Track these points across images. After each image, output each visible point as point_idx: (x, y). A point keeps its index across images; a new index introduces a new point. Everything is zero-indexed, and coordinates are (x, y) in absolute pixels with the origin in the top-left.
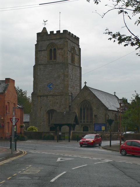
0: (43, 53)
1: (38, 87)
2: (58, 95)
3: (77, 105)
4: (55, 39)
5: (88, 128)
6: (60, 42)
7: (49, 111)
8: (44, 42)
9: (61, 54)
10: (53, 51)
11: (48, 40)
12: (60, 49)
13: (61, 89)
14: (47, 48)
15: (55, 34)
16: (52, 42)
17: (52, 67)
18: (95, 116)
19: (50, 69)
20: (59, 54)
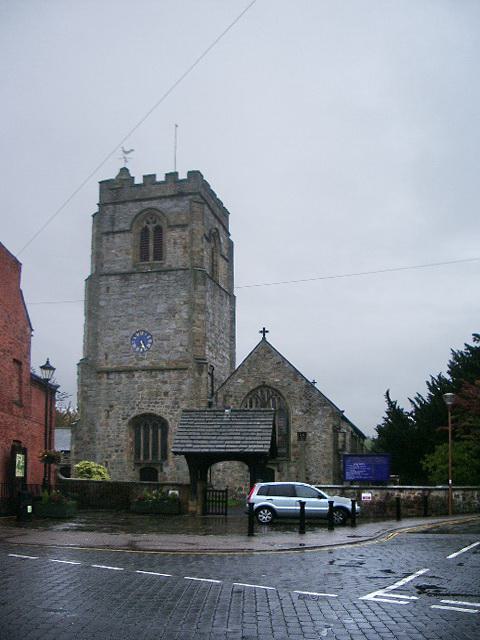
0: (118, 239)
1: (99, 344)
2: (169, 370)
3: (235, 400)
4: (160, 198)
6: (176, 206)
7: (136, 417)
11: (137, 200)
12: (178, 226)
14: (131, 226)
15: (159, 183)
16: (149, 206)
18: (302, 436)
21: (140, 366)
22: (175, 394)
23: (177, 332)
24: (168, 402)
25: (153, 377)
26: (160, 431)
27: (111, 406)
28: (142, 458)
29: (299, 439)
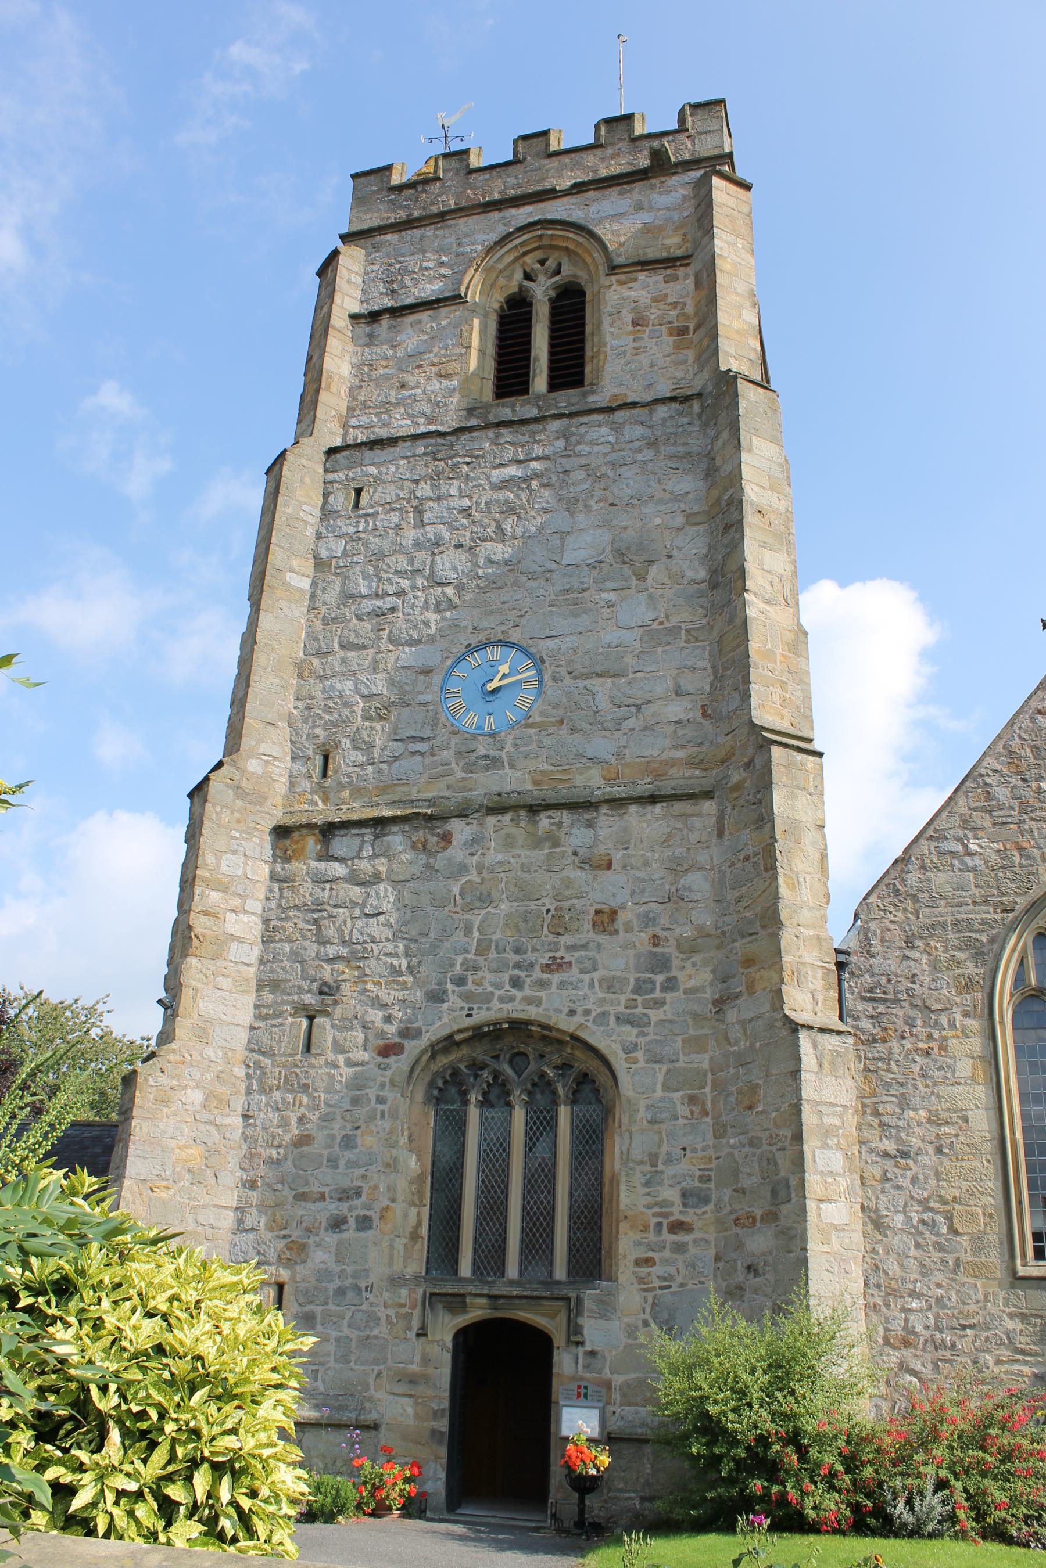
2: (617, 803)
4: (579, 188)
6: (639, 207)
7: (449, 1043)
8: (429, 232)
9: (653, 314)
13: (676, 710)
17: (538, 450)
19: (497, 475)
20: (628, 317)
21: (478, 794)
22: (648, 920)
23: (658, 635)
24: (618, 957)
25: (537, 843)
26: (564, 1113)
27: (327, 990)
28: (466, 1269)
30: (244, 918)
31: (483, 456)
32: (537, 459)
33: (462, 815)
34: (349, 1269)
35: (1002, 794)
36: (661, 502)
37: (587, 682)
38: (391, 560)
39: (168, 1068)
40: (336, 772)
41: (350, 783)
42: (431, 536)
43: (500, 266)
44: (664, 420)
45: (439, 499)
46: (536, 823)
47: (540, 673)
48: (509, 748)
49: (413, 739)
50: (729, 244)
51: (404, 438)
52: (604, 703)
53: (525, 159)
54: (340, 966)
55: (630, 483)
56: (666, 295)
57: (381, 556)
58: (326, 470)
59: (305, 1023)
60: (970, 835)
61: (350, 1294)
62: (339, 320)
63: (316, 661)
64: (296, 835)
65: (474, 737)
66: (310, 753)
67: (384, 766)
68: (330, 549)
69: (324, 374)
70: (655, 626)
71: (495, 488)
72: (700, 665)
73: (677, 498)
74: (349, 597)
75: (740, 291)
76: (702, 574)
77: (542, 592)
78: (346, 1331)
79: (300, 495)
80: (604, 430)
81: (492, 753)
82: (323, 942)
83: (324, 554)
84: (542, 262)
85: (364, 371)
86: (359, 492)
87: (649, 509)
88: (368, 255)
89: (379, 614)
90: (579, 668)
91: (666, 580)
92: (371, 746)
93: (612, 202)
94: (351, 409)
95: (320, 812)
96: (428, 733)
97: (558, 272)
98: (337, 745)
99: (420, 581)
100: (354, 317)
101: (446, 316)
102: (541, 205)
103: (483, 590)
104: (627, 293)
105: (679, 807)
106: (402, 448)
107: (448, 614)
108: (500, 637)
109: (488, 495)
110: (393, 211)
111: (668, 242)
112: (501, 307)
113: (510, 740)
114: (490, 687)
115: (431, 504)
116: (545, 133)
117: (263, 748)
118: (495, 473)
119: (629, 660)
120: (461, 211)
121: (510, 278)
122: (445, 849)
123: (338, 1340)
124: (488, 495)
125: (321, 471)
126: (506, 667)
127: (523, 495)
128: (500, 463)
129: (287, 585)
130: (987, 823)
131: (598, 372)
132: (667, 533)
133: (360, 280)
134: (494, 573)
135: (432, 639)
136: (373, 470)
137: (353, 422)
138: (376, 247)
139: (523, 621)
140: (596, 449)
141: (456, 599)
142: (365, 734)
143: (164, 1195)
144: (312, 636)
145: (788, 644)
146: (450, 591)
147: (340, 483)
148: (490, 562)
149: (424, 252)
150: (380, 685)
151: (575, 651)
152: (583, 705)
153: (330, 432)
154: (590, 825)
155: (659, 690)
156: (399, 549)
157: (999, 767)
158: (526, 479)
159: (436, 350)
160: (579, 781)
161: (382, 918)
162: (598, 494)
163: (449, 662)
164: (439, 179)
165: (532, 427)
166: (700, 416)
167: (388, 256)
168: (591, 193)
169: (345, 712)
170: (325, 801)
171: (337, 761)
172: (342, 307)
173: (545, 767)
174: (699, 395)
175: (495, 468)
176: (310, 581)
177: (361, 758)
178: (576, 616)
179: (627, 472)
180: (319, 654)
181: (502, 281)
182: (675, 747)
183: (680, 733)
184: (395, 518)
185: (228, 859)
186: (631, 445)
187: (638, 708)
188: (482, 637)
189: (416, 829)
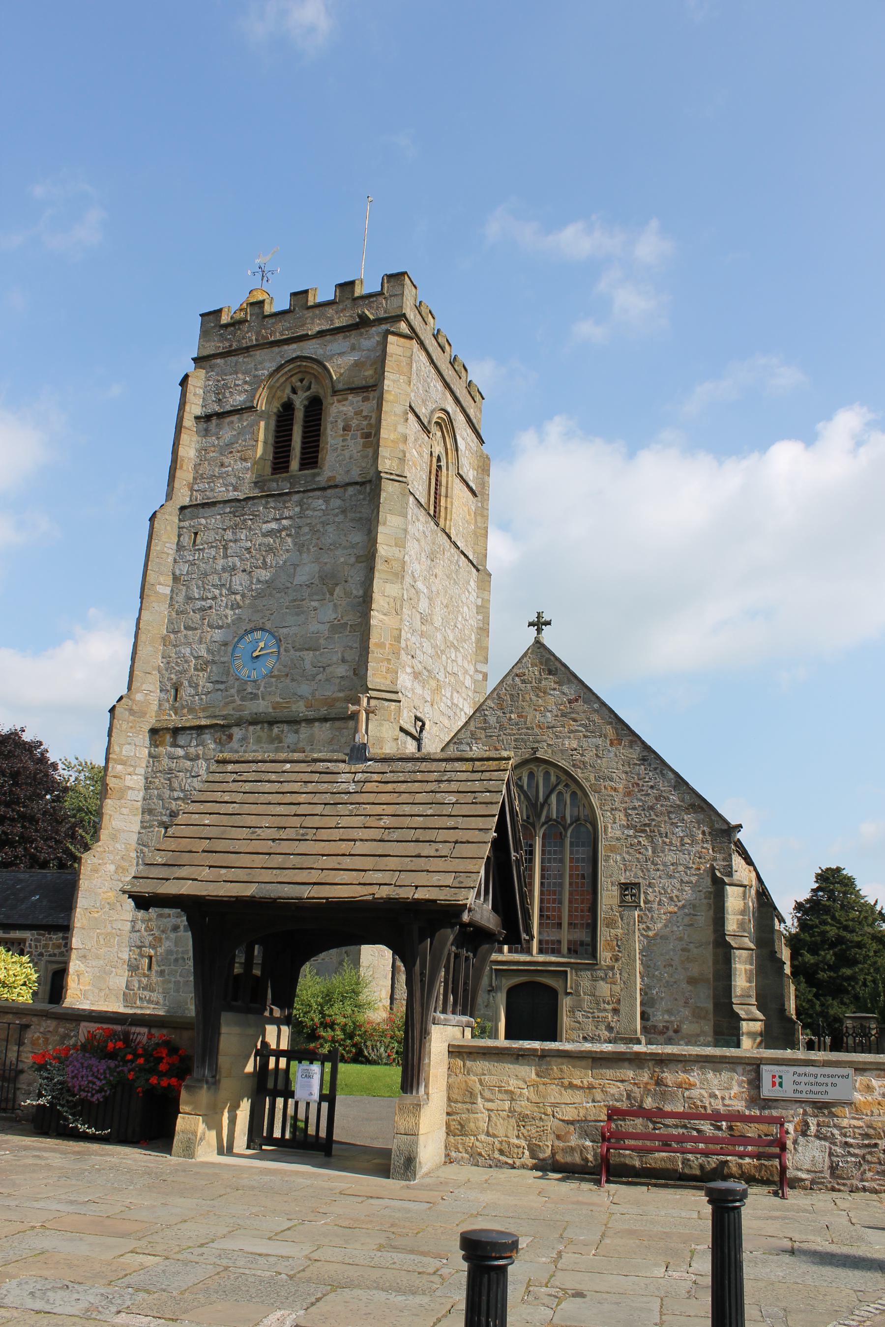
2: (310, 721)
4: (321, 334)
5: (552, 996)
6: (353, 348)
8: (240, 359)
9: (354, 423)
10: (299, 415)
16: (299, 353)
17: (287, 513)
20: (341, 425)
25: (272, 741)
29: (623, 904)
30: (135, 777)
31: (258, 515)
32: (286, 518)
33: (238, 725)
34: (180, 950)
35: (492, 720)
36: (345, 548)
37: (301, 653)
38: (210, 578)
39: (97, 855)
40: (181, 699)
41: (187, 705)
42: (230, 564)
43: (278, 385)
44: (351, 496)
45: (236, 541)
46: (272, 730)
47: (279, 647)
48: (262, 689)
49: (217, 682)
50: (394, 381)
51: (220, 502)
52: (308, 665)
53: (294, 309)
54: (180, 802)
55: (331, 535)
56: (362, 411)
57: (206, 575)
58: (180, 520)
59: (163, 831)
60: (474, 742)
61: (180, 961)
62: (189, 422)
63: (172, 636)
64: (161, 733)
65: (246, 682)
66: (169, 688)
67: (204, 697)
68: (180, 569)
69: (179, 459)
70: (336, 622)
71: (264, 535)
72: (355, 645)
73: (353, 546)
74: (189, 599)
75: (398, 412)
76: (361, 593)
77: (282, 600)
78: (179, 978)
79: (164, 538)
80: (321, 501)
81: (254, 691)
82: (172, 790)
83: (178, 572)
84: (302, 381)
85: (203, 451)
86: (196, 534)
87: (338, 552)
88: (207, 373)
89: (202, 609)
90: (298, 646)
91: (343, 596)
92: (197, 685)
93: (339, 344)
94: (195, 479)
95: (173, 721)
96: (224, 679)
97: (309, 388)
98: (182, 684)
99: (224, 591)
100: (197, 418)
101: (247, 419)
102: (301, 344)
103: (255, 598)
104: (342, 408)
105: (338, 724)
106: (218, 509)
107: (237, 611)
108: (261, 625)
109: (260, 540)
110: (222, 342)
111: (366, 373)
112: (279, 411)
113: (263, 684)
114: (255, 654)
115: (231, 544)
116: (306, 292)
117: (144, 687)
118: (264, 526)
119: (322, 641)
120: (259, 346)
121: (283, 391)
122: (229, 742)
123: (175, 982)
124: (260, 540)
125: (177, 521)
126: (262, 642)
127: (278, 541)
128: (269, 520)
129: (157, 593)
130: (483, 736)
131: (324, 459)
132: (346, 567)
133: (201, 391)
134: (260, 588)
135: (228, 626)
136: (203, 521)
137: (196, 487)
138: (212, 368)
139: (272, 617)
140: (316, 513)
141: (241, 603)
142: (195, 678)
143: (96, 915)
144: (170, 622)
145: (395, 637)
146: (238, 597)
147: (186, 528)
148: (259, 581)
149: (237, 373)
150: (203, 653)
151: (296, 634)
152: (298, 665)
153: (183, 497)
154: (297, 732)
155: (335, 659)
156: (215, 572)
157: (493, 705)
158: (280, 531)
159: (240, 441)
160: (294, 708)
161: (199, 778)
162: (314, 541)
163: (236, 639)
164: (247, 321)
165: (285, 498)
166: (369, 494)
167: (217, 375)
168: (328, 337)
169: (186, 666)
170: (176, 714)
171: (182, 693)
172: (190, 413)
173: (278, 699)
174: (370, 481)
175: (265, 523)
176: (170, 589)
177: (193, 692)
178: (298, 615)
179: (330, 529)
180: (175, 632)
181: (279, 393)
182: (340, 691)
183: (342, 683)
184: (213, 552)
185: (126, 748)
186: (333, 512)
187: (324, 668)
188: (252, 625)
189: (217, 732)
